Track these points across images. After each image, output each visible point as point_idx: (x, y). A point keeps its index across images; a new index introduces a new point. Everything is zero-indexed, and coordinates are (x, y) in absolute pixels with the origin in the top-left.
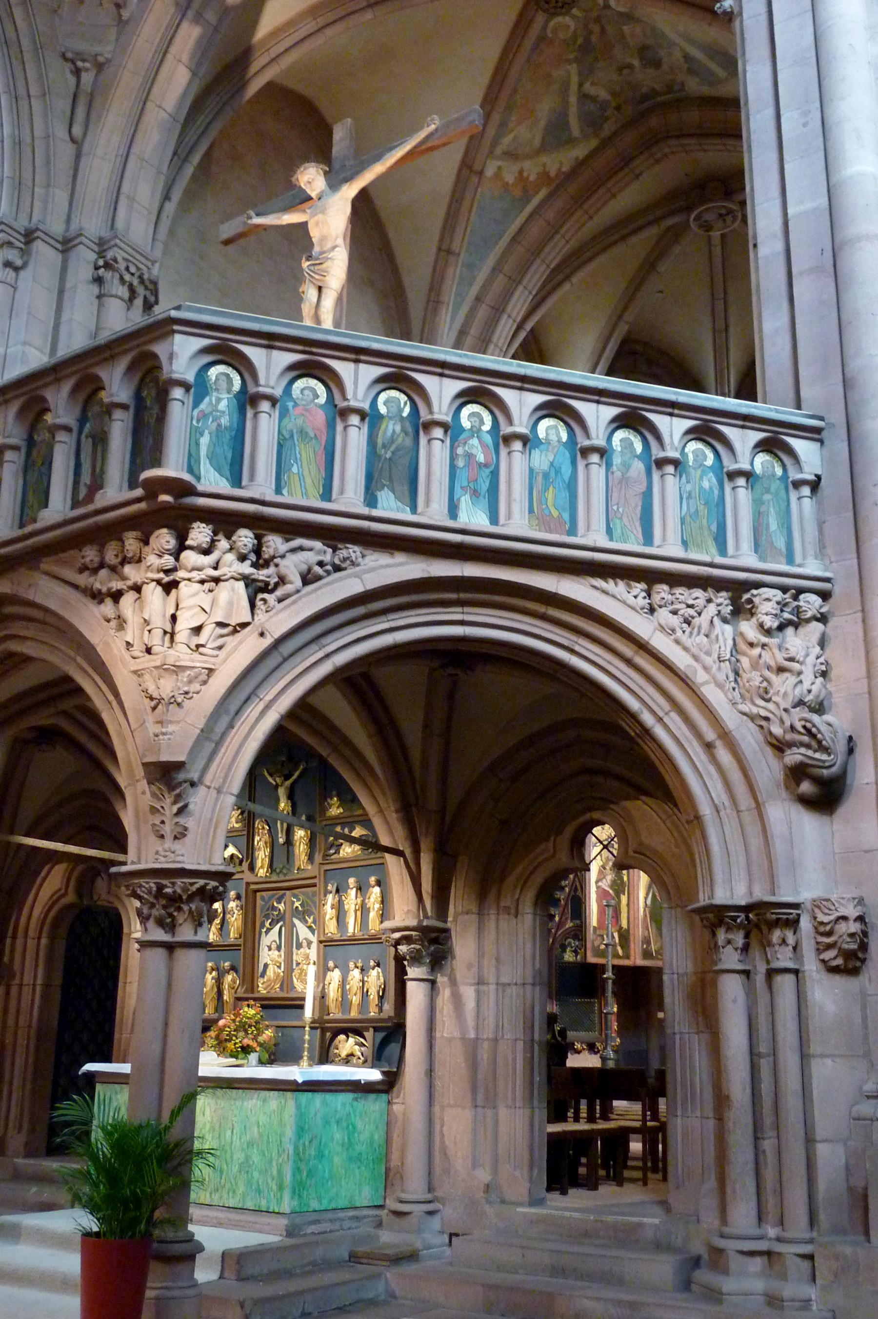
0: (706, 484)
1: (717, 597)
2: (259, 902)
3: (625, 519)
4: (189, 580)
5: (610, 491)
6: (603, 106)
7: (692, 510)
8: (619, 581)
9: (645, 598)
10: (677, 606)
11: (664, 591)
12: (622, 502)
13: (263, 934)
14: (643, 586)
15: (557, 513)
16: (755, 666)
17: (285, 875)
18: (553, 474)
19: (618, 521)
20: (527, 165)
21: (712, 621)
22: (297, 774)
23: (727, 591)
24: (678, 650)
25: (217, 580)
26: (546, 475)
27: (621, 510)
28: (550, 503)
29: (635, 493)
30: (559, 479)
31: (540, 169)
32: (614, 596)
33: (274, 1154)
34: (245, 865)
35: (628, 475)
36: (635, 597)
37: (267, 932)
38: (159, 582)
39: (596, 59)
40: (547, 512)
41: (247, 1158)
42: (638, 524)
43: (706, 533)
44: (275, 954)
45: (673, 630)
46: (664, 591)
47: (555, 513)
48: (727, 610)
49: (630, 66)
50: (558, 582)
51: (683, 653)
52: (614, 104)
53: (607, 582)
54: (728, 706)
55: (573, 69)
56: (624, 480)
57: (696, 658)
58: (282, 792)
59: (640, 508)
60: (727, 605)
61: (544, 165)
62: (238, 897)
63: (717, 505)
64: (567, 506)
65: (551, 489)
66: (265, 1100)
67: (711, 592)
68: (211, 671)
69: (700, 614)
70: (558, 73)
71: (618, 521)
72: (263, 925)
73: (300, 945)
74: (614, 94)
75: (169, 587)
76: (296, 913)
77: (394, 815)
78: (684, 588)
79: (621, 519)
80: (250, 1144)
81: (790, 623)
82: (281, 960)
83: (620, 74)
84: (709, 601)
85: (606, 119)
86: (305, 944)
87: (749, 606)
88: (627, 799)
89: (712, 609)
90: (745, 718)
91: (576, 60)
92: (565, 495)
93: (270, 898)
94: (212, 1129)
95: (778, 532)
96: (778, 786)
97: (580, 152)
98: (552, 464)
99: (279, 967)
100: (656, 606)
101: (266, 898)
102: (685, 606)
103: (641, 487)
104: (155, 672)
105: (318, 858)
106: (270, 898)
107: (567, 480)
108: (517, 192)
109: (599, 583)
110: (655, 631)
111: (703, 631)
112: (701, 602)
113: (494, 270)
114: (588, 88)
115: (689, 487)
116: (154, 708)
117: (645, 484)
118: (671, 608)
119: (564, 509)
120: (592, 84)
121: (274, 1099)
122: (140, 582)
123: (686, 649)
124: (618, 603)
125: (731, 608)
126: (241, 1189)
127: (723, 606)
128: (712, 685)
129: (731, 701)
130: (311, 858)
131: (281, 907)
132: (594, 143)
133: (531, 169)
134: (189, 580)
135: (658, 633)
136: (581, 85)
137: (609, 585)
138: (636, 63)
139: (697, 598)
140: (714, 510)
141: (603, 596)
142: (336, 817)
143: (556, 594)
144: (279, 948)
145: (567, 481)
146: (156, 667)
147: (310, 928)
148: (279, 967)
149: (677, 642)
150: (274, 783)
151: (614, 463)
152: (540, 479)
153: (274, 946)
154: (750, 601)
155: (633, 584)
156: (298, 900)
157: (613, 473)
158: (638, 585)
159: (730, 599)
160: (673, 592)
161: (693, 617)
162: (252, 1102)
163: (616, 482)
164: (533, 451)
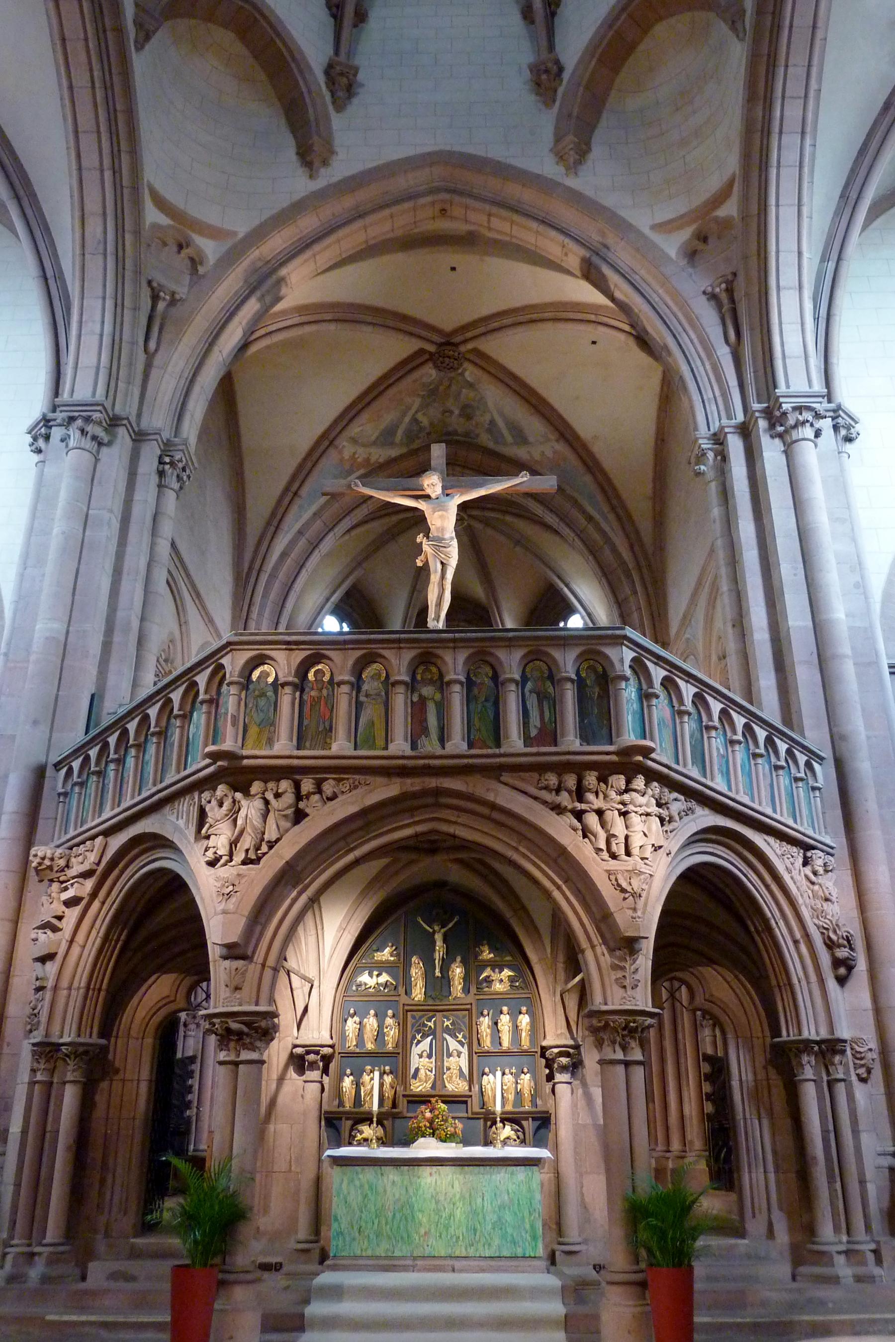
2: (410, 1020)
4: (636, 812)
6: (421, 429)
13: (414, 1045)
17: (441, 1000)
20: (360, 450)
22: (450, 925)
25: (648, 815)
31: (366, 456)
33: (526, 1214)
34: (401, 990)
37: (419, 1042)
38: (619, 810)
39: (434, 401)
41: (500, 1219)
44: (425, 1060)
49: (451, 412)
52: (428, 431)
55: (417, 402)
58: (439, 938)
61: (370, 454)
62: (394, 1016)
66: (512, 1174)
68: (651, 875)
70: (408, 400)
72: (414, 1037)
73: (450, 1055)
74: (431, 424)
75: (624, 814)
76: (447, 1030)
77: (562, 965)
80: (502, 1207)
82: (433, 1065)
83: (443, 415)
85: (419, 438)
86: (455, 1053)
88: (700, 966)
91: (423, 397)
93: (421, 1017)
94: (462, 1197)
97: (394, 453)
99: (431, 1071)
101: (417, 1017)
104: (626, 874)
105: (473, 990)
106: (421, 1017)
108: (347, 466)
113: (315, 514)
114: (420, 416)
116: (625, 899)
120: (424, 414)
121: (521, 1173)
122: (604, 808)
126: (496, 1242)
130: (466, 990)
131: (431, 1024)
132: (404, 450)
133: (362, 453)
134: (636, 812)
136: (416, 412)
138: (457, 412)
142: (489, 961)
144: (430, 1056)
146: (627, 871)
147: (460, 1042)
148: (431, 1071)
150: (431, 930)
153: (425, 1054)
156: (448, 1020)
162: (500, 1176)
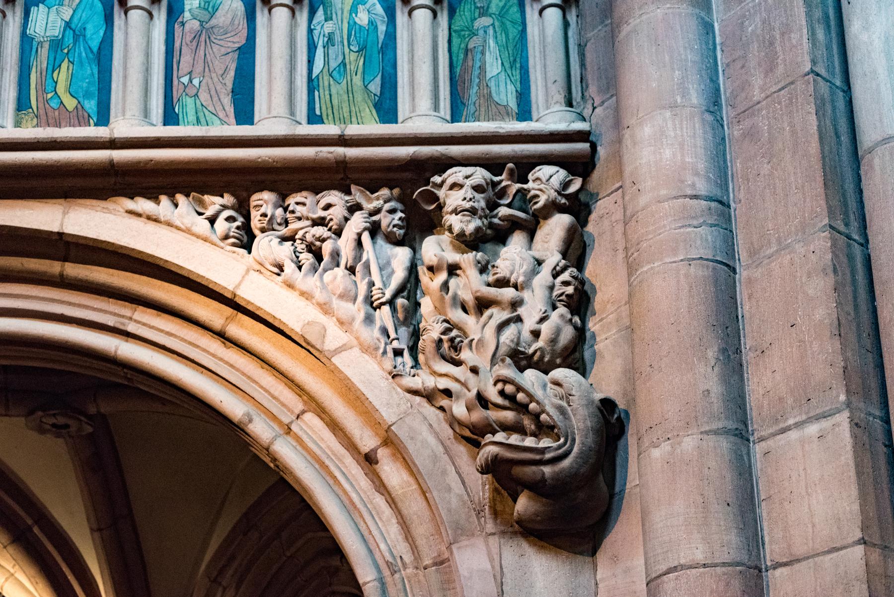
0: (363, 18)
1: (370, 200)
3: (204, 96)
5: (176, 53)
7: (333, 64)
8: (180, 198)
9: (230, 219)
10: (292, 226)
11: (266, 202)
12: (199, 68)
14: (228, 199)
15: (75, 102)
16: (439, 309)
18: (69, 40)
19: (190, 102)
21: (359, 243)
23: (391, 189)
24: (291, 297)
26: (56, 44)
27: (196, 82)
28: (61, 89)
29: (223, 51)
30: (81, 48)
32: (169, 224)
35: (213, 22)
36: (212, 220)
40: (54, 104)
42: (227, 101)
43: (359, 97)
45: (281, 268)
46: (266, 202)
47: (70, 103)
48: (390, 221)
50: (65, 213)
51: (302, 302)
53: (158, 203)
54: (385, 383)
56: (205, 33)
57: (325, 308)
59: (232, 73)
60: (392, 211)
63: (383, 50)
64: (94, 89)
65: (65, 65)
67: (358, 195)
69: (338, 233)
71: (190, 102)
78: (304, 193)
79: (196, 95)
81: (513, 225)
84: (354, 208)
87: (433, 207)
89: (358, 222)
90: (418, 399)
92: (91, 70)
95: (503, 76)
96: (479, 513)
98: (68, 25)
100: (256, 232)
102: (309, 223)
103: (236, 39)
107: (95, 44)
109: (143, 205)
110: (248, 271)
111: (343, 263)
112: (337, 213)
115: (329, 27)
117: (245, 33)
118: (284, 231)
119: (87, 95)
123: (304, 294)
124: (180, 235)
125: (400, 214)
127: (383, 213)
128: (356, 351)
129: (390, 373)
135: (254, 275)
137: (163, 207)
139: (328, 207)
140: (376, 58)
141: (151, 226)
143: (61, 235)
145: (95, 50)
149: (290, 286)
151: (187, 7)
152: (44, 52)
154: (435, 198)
155: (207, 198)
157: (183, 24)
158: (218, 200)
159: (400, 199)
160: (286, 204)
161: (323, 240)
163: (188, 38)
164: (34, 10)
